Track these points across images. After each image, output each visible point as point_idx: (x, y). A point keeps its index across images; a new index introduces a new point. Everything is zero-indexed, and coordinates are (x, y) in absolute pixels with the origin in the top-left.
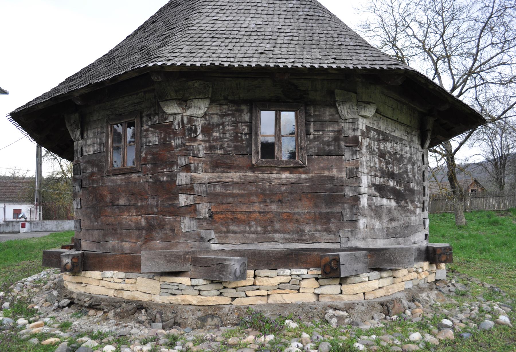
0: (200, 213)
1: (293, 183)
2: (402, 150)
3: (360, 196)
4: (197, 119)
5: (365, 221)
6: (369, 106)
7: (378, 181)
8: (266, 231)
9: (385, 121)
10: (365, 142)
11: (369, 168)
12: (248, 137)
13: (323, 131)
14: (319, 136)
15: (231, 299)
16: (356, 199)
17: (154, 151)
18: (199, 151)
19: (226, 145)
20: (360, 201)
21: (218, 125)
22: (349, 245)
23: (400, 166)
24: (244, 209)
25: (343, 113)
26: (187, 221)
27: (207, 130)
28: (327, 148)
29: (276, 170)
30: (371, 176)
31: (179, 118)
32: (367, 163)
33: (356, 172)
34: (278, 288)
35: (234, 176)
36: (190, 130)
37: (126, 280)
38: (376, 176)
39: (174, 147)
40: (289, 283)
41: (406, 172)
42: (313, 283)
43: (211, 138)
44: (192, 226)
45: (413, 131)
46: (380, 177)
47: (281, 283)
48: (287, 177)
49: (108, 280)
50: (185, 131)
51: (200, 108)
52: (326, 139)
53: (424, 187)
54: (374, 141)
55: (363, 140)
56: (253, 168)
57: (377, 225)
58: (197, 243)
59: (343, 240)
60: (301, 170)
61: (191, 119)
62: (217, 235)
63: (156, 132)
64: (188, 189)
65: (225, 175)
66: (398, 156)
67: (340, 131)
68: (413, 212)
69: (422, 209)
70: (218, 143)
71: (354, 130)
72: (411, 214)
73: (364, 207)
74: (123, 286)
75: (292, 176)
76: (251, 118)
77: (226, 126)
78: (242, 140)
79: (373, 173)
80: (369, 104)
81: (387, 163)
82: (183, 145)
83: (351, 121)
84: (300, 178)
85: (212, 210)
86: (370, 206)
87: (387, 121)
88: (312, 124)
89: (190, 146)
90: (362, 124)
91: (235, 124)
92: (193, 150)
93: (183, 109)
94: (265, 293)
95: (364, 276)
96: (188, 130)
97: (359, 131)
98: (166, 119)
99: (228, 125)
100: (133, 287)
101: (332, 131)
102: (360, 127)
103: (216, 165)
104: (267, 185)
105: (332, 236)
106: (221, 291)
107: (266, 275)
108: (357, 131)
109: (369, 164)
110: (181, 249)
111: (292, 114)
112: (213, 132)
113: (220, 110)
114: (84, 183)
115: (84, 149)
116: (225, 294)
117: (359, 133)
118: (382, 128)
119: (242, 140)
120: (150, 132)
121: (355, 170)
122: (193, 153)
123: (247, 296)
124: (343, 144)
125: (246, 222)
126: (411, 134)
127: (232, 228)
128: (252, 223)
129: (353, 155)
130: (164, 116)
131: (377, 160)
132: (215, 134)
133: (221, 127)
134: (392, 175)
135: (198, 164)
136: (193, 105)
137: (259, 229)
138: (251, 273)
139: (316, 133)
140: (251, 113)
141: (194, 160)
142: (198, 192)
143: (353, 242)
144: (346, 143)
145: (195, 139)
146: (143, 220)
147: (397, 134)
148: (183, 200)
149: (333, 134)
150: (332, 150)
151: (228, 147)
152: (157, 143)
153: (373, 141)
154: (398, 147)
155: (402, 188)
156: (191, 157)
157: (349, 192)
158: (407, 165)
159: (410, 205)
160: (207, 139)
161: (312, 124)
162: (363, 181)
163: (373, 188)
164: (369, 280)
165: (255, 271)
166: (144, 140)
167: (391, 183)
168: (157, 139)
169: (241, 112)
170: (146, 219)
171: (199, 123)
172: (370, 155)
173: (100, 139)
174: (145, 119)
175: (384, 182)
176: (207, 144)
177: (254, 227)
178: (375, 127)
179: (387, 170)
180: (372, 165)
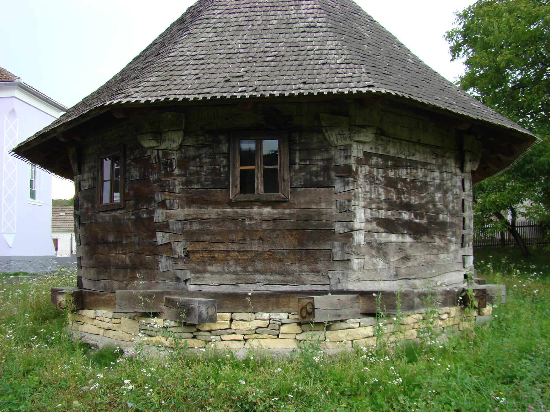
0: (176, 253)
1: (275, 219)
2: (425, 176)
3: (353, 232)
4: (173, 152)
5: (362, 260)
6: (364, 130)
7: (383, 214)
8: (245, 272)
9: (398, 145)
10: (364, 170)
11: (368, 200)
12: (226, 169)
13: (311, 160)
14: (305, 166)
15: (204, 343)
16: (349, 235)
17: (136, 186)
18: (175, 186)
19: (203, 179)
20: (354, 239)
21: (194, 158)
22: (340, 287)
23: (422, 195)
24: (222, 247)
25: (332, 139)
26: (163, 260)
27: (183, 164)
28: (314, 179)
29: (256, 205)
30: (371, 209)
31: (155, 152)
32: (365, 195)
33: (349, 206)
34: (256, 333)
35: (212, 213)
36: (166, 164)
37: (113, 319)
38: (379, 208)
39: (152, 182)
40: (268, 327)
41: (433, 202)
42: (293, 328)
43: (188, 172)
44: (168, 265)
45: (446, 153)
46: (387, 210)
47: (258, 328)
48: (269, 213)
49: (99, 318)
50: (160, 165)
51: (174, 141)
52: (314, 169)
53: (464, 218)
54: (378, 168)
55: (359, 169)
56: (232, 204)
57: (381, 264)
58: (173, 284)
59: (333, 282)
60: (285, 204)
61: (166, 152)
62: (193, 275)
63: (137, 167)
64: (165, 227)
65: (203, 211)
66: (419, 184)
67: (330, 160)
68: (446, 249)
69: (460, 245)
70: (194, 177)
71: (346, 158)
72: (439, 250)
73: (359, 245)
74: (110, 325)
75: (275, 211)
76: (229, 150)
77: (202, 158)
78: (221, 173)
79: (374, 206)
80: (365, 128)
81: (399, 193)
82: (159, 180)
83: (342, 148)
84: (283, 214)
85: (188, 249)
86: (368, 243)
87: (400, 144)
88: (298, 153)
89: (166, 181)
90: (357, 151)
91: (212, 157)
92: (169, 186)
93: (158, 142)
94: (241, 337)
95: (353, 322)
96: (164, 164)
97: (353, 158)
98: (145, 152)
99: (205, 157)
100: (118, 327)
101: (321, 160)
102: (354, 153)
103: (190, 201)
104: (247, 221)
105: (321, 278)
106: (195, 334)
107: (242, 318)
108: (350, 158)
109: (368, 196)
110: (160, 288)
111: (276, 142)
112: (190, 166)
113: (196, 141)
114: (82, 218)
115: (82, 184)
116: (199, 337)
117: (352, 161)
118: (392, 152)
119: (221, 173)
120: (132, 167)
121: (347, 203)
122: (169, 189)
123: (222, 340)
124: (333, 174)
125: (226, 262)
126: (443, 156)
127: (209, 268)
128: (231, 262)
129: (344, 186)
130: (143, 150)
131: (381, 190)
132: (191, 168)
133: (198, 160)
134: (408, 207)
135: (174, 200)
136: (167, 138)
137: (239, 269)
138: (228, 316)
139: (302, 163)
140: (229, 144)
141: (170, 196)
142: (173, 231)
143: (344, 285)
144: (337, 172)
145: (170, 174)
146: (127, 259)
147: (418, 158)
148: (161, 238)
149: (321, 163)
150: (321, 181)
151: (206, 180)
152: (138, 178)
153: (375, 169)
154: (420, 173)
155: (425, 221)
156: (167, 193)
157: (339, 228)
158: (434, 193)
159: (437, 240)
160: (183, 173)
161: (298, 153)
162: (358, 216)
163: (375, 223)
164: (359, 327)
165: (232, 313)
166: (127, 174)
167: (406, 216)
168: (138, 174)
169: (219, 142)
170: (130, 257)
171: (175, 156)
172: (371, 185)
173: (93, 174)
174: (128, 153)
175: (392, 215)
176: (184, 179)
177: (233, 267)
178: (380, 153)
179: (398, 201)
180: (373, 196)
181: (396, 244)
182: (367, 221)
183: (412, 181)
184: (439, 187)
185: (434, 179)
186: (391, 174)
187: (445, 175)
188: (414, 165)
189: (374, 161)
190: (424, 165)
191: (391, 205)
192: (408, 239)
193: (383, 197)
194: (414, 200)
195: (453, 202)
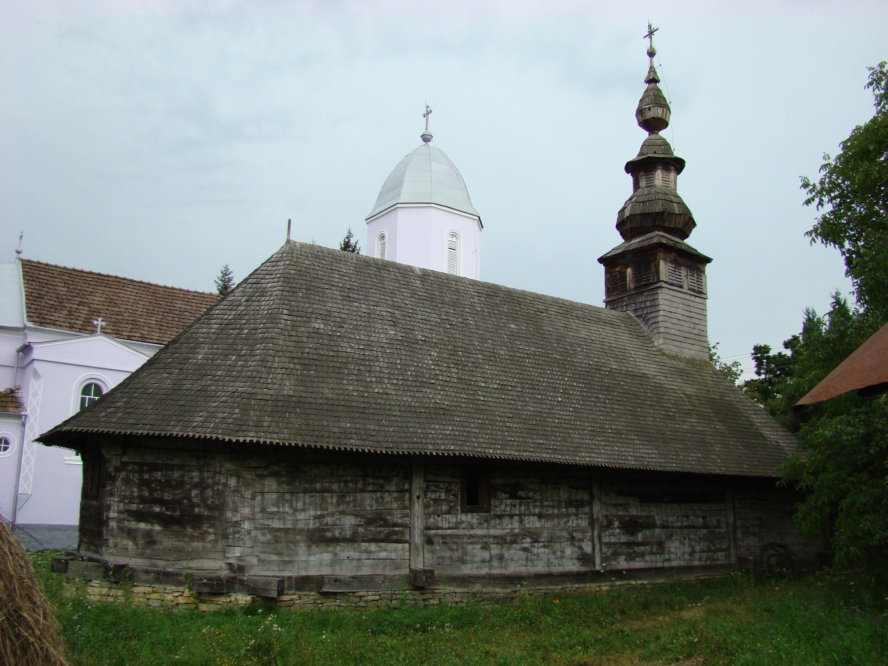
7: (134, 507)
30: (125, 503)
41: (189, 499)
68: (202, 537)
73: (113, 528)
81: (152, 491)
90: (116, 462)
118: (149, 459)
131: (135, 489)
134: (160, 502)
147: (176, 461)
154: (176, 474)
155: (178, 513)
158: (190, 490)
159: (190, 530)
167: (157, 509)
181: (145, 531)
182: (119, 512)
183: (167, 481)
184: (196, 486)
185: (192, 478)
186: (146, 476)
187: (206, 474)
188: (172, 468)
189: (130, 467)
190: (181, 467)
191: (143, 500)
192: (157, 528)
193: (136, 494)
194: (167, 496)
195: (212, 497)
